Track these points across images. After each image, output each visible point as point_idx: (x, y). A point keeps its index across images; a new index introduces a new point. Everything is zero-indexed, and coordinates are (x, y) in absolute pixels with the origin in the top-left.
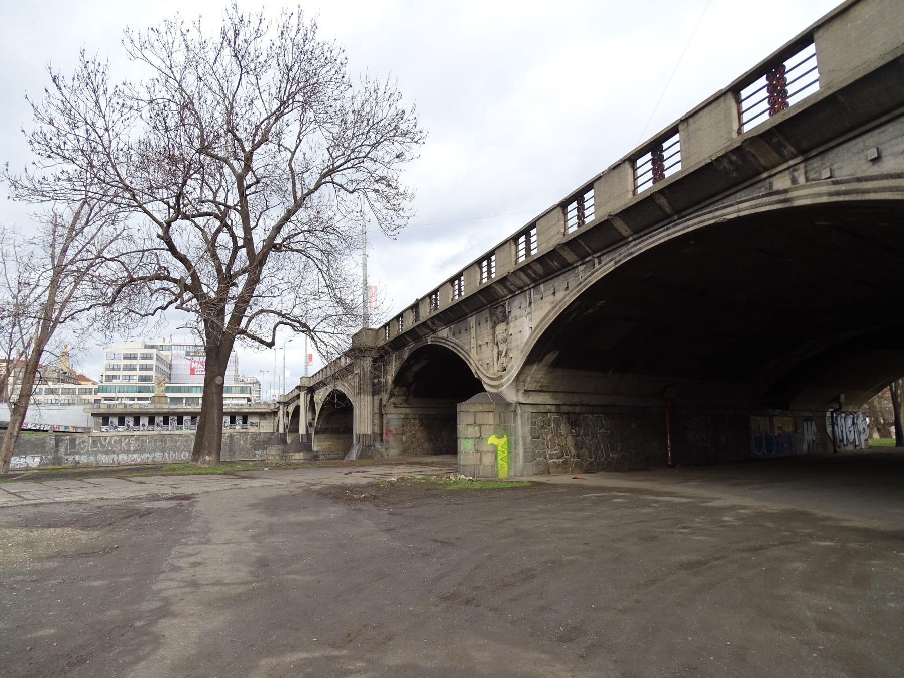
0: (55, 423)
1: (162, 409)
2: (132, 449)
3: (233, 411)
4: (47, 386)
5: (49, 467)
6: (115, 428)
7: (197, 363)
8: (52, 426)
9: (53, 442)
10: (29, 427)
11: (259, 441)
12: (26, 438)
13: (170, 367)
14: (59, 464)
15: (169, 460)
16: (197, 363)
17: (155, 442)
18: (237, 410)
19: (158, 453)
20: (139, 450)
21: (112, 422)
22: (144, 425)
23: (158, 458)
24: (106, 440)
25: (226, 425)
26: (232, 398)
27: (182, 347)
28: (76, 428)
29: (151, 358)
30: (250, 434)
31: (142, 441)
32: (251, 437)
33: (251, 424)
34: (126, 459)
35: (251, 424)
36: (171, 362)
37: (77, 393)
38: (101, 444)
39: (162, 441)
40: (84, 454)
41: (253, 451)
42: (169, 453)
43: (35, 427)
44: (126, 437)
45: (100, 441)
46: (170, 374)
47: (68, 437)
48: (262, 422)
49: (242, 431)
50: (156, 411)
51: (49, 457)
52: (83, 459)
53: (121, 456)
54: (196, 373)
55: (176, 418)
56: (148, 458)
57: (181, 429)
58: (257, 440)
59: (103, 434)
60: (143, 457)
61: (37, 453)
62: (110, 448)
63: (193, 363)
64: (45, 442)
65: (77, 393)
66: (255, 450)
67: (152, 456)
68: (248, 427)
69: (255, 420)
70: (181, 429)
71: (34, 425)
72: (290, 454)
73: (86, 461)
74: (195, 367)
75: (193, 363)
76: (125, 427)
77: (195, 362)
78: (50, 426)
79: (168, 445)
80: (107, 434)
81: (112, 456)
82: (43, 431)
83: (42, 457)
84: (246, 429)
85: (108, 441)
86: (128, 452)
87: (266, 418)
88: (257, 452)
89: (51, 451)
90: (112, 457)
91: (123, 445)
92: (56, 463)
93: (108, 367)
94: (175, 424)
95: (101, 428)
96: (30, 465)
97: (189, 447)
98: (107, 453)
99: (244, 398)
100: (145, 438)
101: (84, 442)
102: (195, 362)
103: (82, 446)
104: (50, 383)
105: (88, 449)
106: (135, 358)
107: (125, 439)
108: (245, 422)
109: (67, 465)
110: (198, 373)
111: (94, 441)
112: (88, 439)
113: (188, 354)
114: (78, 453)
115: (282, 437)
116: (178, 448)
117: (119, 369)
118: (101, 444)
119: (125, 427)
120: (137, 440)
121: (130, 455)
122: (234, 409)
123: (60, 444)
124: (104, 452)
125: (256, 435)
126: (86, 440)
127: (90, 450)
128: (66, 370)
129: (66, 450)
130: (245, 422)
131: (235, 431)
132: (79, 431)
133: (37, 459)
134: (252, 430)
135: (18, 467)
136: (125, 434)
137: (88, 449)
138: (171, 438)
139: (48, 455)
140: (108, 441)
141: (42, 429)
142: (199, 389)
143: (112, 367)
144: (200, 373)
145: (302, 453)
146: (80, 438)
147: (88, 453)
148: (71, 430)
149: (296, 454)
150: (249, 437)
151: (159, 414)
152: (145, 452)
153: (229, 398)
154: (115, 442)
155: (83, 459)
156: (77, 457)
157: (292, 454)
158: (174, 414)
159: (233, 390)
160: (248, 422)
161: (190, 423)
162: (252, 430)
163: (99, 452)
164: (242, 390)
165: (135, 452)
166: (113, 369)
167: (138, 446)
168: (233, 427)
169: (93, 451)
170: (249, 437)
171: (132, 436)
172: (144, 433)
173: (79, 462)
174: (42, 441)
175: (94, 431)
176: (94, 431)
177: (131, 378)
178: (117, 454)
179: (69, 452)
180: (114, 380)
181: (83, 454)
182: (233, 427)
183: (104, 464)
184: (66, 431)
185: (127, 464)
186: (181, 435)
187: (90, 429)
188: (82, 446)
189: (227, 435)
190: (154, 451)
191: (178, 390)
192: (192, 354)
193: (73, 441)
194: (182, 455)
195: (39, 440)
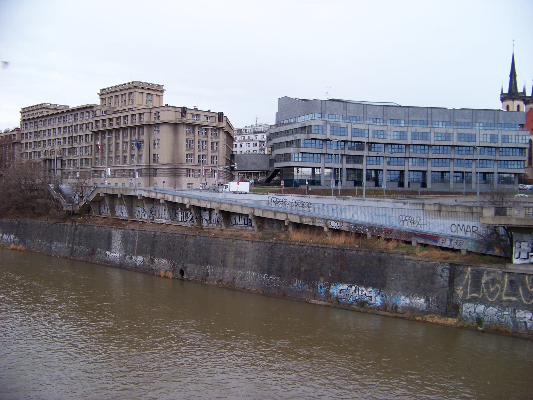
38: (525, 290)
45: (524, 284)
64: (434, 274)
105: (500, 296)
111: (511, 282)
114: (482, 301)
123: (456, 280)
126: (499, 278)
127: (504, 298)
129: (465, 293)
147: (499, 303)
163: (516, 306)
169: (510, 301)
174: (431, 271)
179: (469, 297)
188: (492, 290)
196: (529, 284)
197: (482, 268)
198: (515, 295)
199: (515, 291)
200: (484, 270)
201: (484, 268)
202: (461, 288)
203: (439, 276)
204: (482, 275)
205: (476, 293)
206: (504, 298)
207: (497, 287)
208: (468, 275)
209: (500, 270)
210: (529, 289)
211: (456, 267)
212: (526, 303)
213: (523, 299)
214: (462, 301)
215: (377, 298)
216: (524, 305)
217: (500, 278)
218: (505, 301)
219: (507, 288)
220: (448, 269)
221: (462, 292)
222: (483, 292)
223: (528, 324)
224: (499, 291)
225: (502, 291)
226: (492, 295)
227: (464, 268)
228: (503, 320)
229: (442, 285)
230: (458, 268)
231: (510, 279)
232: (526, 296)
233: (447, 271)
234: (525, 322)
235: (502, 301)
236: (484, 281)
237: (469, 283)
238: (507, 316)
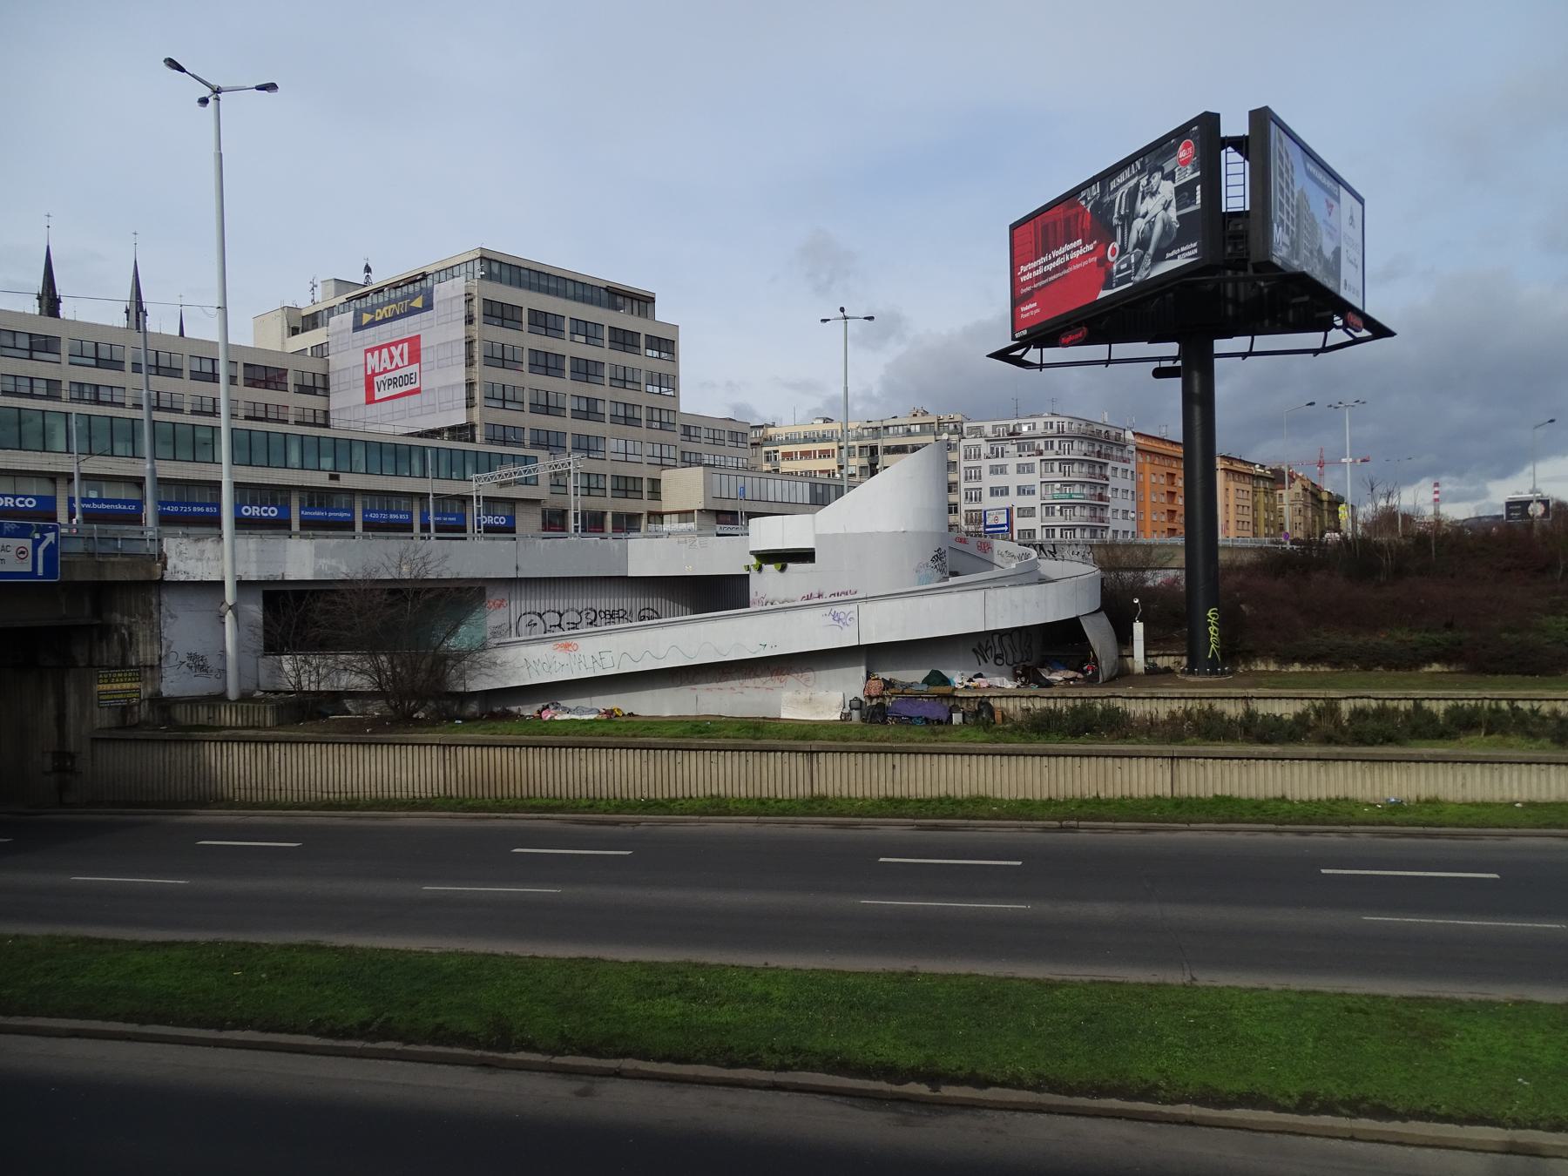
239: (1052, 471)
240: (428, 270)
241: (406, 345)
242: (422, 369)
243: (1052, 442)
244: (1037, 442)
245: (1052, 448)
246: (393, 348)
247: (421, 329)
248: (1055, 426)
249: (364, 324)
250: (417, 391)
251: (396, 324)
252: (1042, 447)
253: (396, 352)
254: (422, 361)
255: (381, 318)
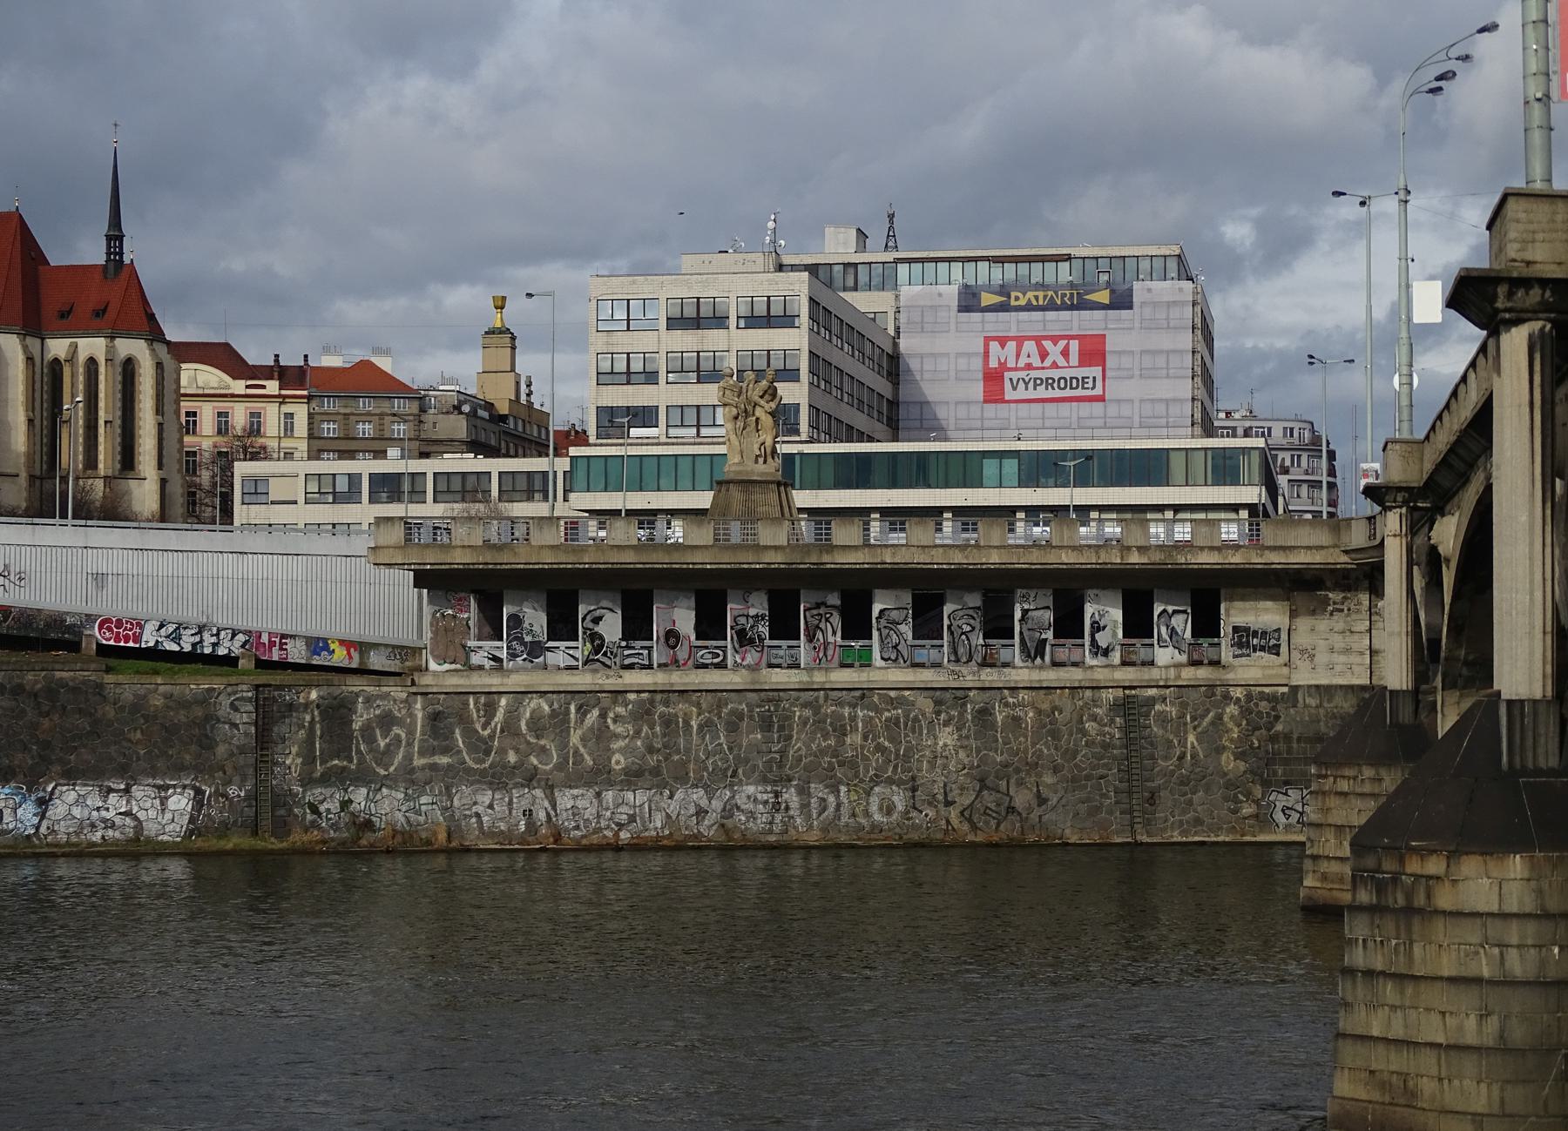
0: (267, 623)
1: (759, 548)
2: (618, 761)
3: (1135, 558)
4: (380, 467)
5: (232, 842)
6: (536, 650)
7: (1011, 345)
8: (253, 637)
9: (245, 717)
10: (149, 639)
11: (1287, 737)
12: (128, 695)
13: (893, 365)
14: (282, 828)
15: (806, 830)
16: (1011, 345)
17: (732, 728)
18: (1157, 557)
19: (751, 789)
20: (656, 772)
21: (516, 620)
22: (672, 637)
23: (752, 815)
24: (490, 709)
25: (1103, 639)
26: (1177, 508)
27: (943, 266)
28: (363, 647)
29: (787, 321)
30: (1238, 693)
31: (668, 722)
32: (1245, 712)
33: (1245, 639)
34: (590, 813)
35: (1245, 639)
36: (895, 345)
37: (495, 492)
38: (469, 732)
39: (767, 725)
40: (390, 782)
41: (1258, 791)
42: (803, 791)
43: (177, 639)
44: (586, 699)
45: (464, 720)
46: (894, 404)
47: (314, 695)
48: (1303, 624)
49: (1189, 674)
50: (726, 560)
51: (232, 791)
52: (385, 807)
53: (565, 800)
54: (1009, 394)
55: (834, 599)
56: (701, 813)
57: (867, 664)
58: (1279, 727)
59: (478, 681)
60: (673, 807)
61: (178, 769)
62: (512, 758)
63: (994, 346)
64: (211, 719)
65: (495, 492)
66: (1266, 784)
67: (717, 805)
68: (1226, 653)
69: (1265, 614)
70: (867, 664)
71: (171, 628)
72: (1414, 866)
73: (399, 816)
74: (1003, 367)
75: (994, 346)
76: (582, 648)
77: (1003, 341)
78: (241, 638)
79: (798, 745)
80: (494, 682)
81: (523, 798)
82: (213, 660)
83: (199, 792)
84: (1216, 663)
85: (500, 716)
86: (598, 777)
87: (1326, 601)
88: (1281, 801)
89: (241, 760)
90: (525, 804)
91: (575, 738)
92: (266, 822)
93: (605, 366)
94: (832, 632)
95: (467, 651)
96: (151, 829)
97: (907, 757)
98: (498, 778)
99: (1235, 508)
100: (681, 707)
101: (387, 721)
102: (1003, 341)
103: (382, 744)
104: (393, 452)
105: (408, 758)
106: (719, 321)
107: (583, 711)
108: (1206, 625)
109: (315, 835)
110: (1021, 393)
111: (434, 718)
112: (408, 703)
113: (969, 301)
114: (363, 777)
115: (1405, 715)
116: (852, 764)
117: (651, 377)
118: (469, 732)
119: (582, 648)
120: (643, 713)
121: (609, 796)
122: (1142, 549)
124: (483, 773)
125: (1272, 699)
127: (418, 762)
128: (503, 409)
129: (309, 759)
130: (1206, 625)
131: (1154, 674)
132: (377, 661)
133: (180, 802)
134: (1251, 670)
135: (97, 837)
136: (583, 680)
137: (408, 758)
138: (814, 706)
139: (229, 783)
140: (500, 716)
141: (207, 651)
142: (1011, 466)
143: (621, 366)
144: (1031, 394)
145: (1516, 865)
146: (369, 700)
148: (339, 656)
149: (1470, 866)
150: (1232, 709)
151: (747, 580)
152: (682, 779)
153: (1160, 508)
154: (536, 725)
155: (385, 807)
156: (359, 796)
157: (1435, 866)
158: (823, 578)
159: (1177, 464)
160: (1225, 629)
161: (906, 630)
162: (1251, 670)
164: (1224, 468)
165: (632, 778)
166: (629, 377)
167: (651, 750)
168: (1143, 654)
169: (434, 767)
170: (1232, 709)
171: (617, 693)
172: (677, 679)
173: (368, 825)
174: (199, 712)
175: (433, 666)
176: (433, 666)
177: (706, 418)
178: (550, 789)
180: (634, 432)
181: (385, 782)
182: (1143, 654)
183: (491, 834)
184: (316, 661)
185: (595, 839)
186: (863, 694)
187: (415, 651)
188: (382, 744)
189: (1109, 696)
190: (729, 776)
191: (919, 470)
192: (988, 299)
193: (337, 713)
194: (874, 803)
195: (183, 704)
196: (479, 717)
197: (351, 689)
198: (445, 751)
199: (446, 739)
200: (357, 695)
201: (355, 689)
202: (294, 750)
203: (224, 723)
204: (352, 711)
205: (338, 757)
206: (418, 762)
207: (398, 736)
208: (312, 711)
209: (399, 689)
210: (480, 730)
211: (276, 693)
212: (476, 767)
213: (467, 758)
214: (301, 786)
215: (20, 812)
216: (469, 771)
217: (404, 712)
218: (423, 768)
219: (423, 734)
220: (249, 700)
221: (299, 761)
222: (359, 752)
223: (485, 819)
224: (404, 743)
225: (410, 744)
226: (385, 757)
227: (298, 693)
228: (422, 819)
229: (238, 747)
230: (280, 696)
231: (430, 709)
232: (472, 748)
233: (251, 708)
234: (478, 815)
235: (412, 771)
236: (360, 724)
237: (318, 733)
238: (430, 807)
239: (1298, 496)
240: (1074, 252)
241: (1074, 346)
242: (1108, 374)
243: (1299, 456)
244: (1281, 455)
245: (1299, 465)
246: (1047, 344)
247: (1106, 328)
248: (1296, 434)
249: (983, 305)
250: (1101, 399)
251: (1051, 315)
252: (1288, 463)
253: (1054, 351)
254: (1109, 364)
255: (1022, 302)
